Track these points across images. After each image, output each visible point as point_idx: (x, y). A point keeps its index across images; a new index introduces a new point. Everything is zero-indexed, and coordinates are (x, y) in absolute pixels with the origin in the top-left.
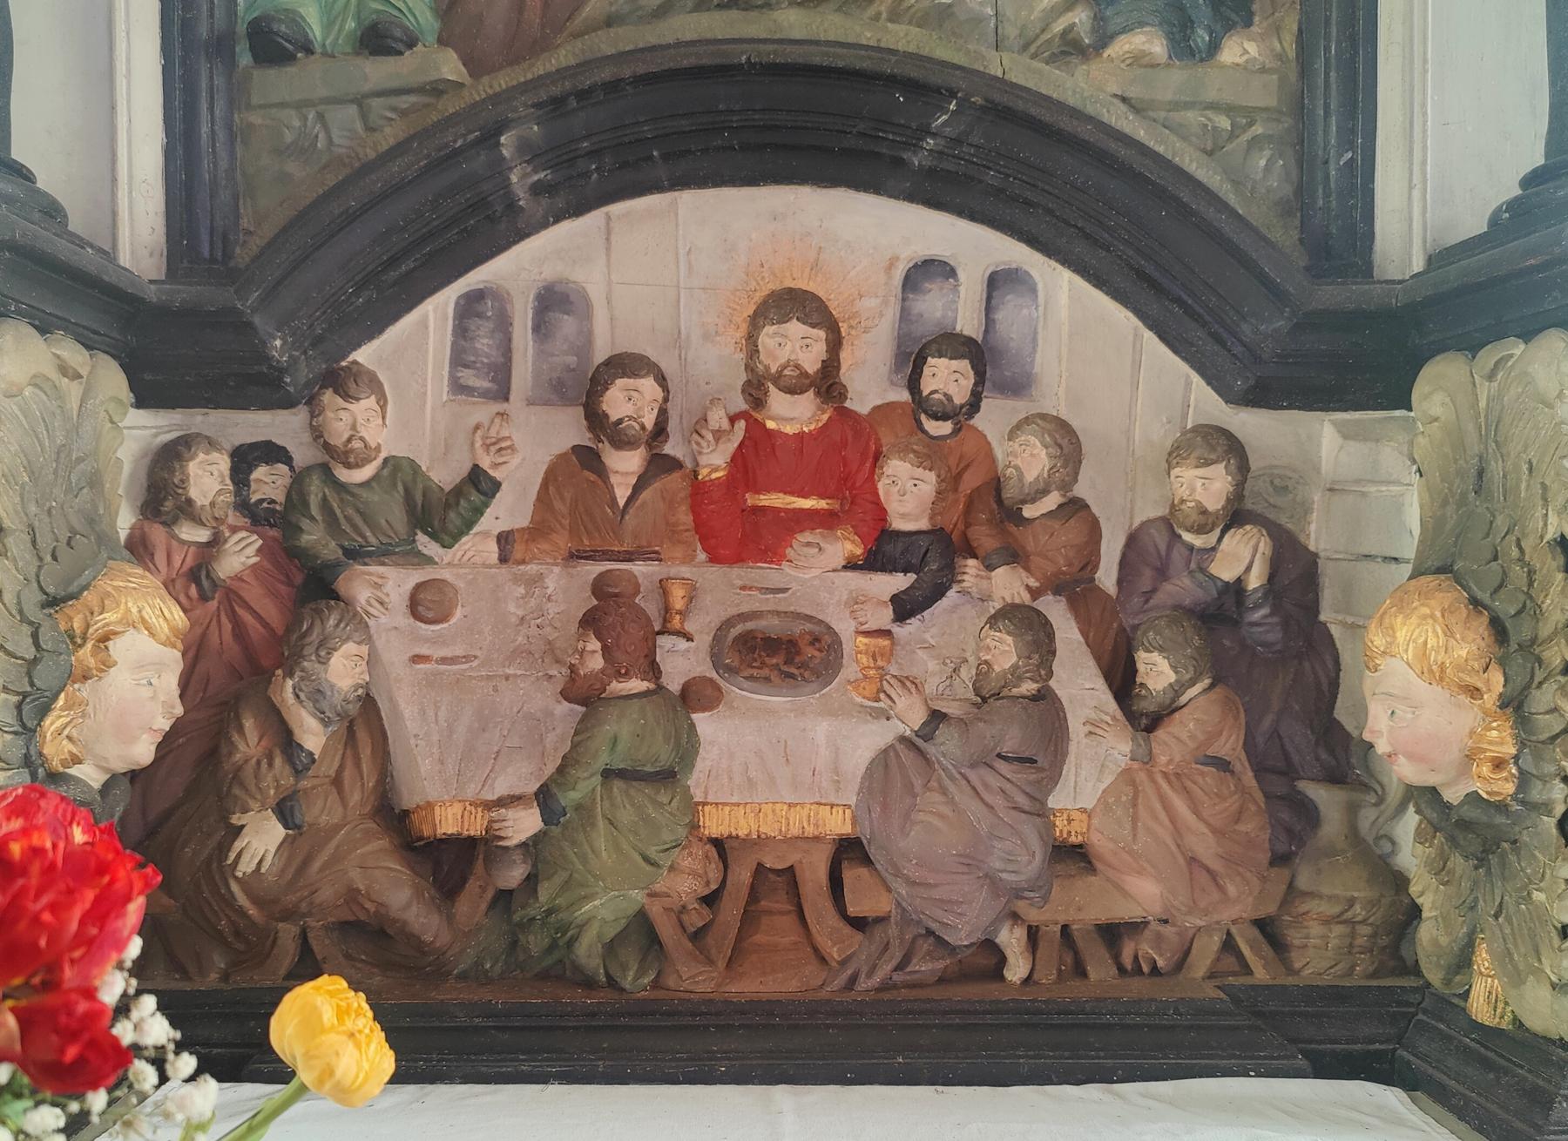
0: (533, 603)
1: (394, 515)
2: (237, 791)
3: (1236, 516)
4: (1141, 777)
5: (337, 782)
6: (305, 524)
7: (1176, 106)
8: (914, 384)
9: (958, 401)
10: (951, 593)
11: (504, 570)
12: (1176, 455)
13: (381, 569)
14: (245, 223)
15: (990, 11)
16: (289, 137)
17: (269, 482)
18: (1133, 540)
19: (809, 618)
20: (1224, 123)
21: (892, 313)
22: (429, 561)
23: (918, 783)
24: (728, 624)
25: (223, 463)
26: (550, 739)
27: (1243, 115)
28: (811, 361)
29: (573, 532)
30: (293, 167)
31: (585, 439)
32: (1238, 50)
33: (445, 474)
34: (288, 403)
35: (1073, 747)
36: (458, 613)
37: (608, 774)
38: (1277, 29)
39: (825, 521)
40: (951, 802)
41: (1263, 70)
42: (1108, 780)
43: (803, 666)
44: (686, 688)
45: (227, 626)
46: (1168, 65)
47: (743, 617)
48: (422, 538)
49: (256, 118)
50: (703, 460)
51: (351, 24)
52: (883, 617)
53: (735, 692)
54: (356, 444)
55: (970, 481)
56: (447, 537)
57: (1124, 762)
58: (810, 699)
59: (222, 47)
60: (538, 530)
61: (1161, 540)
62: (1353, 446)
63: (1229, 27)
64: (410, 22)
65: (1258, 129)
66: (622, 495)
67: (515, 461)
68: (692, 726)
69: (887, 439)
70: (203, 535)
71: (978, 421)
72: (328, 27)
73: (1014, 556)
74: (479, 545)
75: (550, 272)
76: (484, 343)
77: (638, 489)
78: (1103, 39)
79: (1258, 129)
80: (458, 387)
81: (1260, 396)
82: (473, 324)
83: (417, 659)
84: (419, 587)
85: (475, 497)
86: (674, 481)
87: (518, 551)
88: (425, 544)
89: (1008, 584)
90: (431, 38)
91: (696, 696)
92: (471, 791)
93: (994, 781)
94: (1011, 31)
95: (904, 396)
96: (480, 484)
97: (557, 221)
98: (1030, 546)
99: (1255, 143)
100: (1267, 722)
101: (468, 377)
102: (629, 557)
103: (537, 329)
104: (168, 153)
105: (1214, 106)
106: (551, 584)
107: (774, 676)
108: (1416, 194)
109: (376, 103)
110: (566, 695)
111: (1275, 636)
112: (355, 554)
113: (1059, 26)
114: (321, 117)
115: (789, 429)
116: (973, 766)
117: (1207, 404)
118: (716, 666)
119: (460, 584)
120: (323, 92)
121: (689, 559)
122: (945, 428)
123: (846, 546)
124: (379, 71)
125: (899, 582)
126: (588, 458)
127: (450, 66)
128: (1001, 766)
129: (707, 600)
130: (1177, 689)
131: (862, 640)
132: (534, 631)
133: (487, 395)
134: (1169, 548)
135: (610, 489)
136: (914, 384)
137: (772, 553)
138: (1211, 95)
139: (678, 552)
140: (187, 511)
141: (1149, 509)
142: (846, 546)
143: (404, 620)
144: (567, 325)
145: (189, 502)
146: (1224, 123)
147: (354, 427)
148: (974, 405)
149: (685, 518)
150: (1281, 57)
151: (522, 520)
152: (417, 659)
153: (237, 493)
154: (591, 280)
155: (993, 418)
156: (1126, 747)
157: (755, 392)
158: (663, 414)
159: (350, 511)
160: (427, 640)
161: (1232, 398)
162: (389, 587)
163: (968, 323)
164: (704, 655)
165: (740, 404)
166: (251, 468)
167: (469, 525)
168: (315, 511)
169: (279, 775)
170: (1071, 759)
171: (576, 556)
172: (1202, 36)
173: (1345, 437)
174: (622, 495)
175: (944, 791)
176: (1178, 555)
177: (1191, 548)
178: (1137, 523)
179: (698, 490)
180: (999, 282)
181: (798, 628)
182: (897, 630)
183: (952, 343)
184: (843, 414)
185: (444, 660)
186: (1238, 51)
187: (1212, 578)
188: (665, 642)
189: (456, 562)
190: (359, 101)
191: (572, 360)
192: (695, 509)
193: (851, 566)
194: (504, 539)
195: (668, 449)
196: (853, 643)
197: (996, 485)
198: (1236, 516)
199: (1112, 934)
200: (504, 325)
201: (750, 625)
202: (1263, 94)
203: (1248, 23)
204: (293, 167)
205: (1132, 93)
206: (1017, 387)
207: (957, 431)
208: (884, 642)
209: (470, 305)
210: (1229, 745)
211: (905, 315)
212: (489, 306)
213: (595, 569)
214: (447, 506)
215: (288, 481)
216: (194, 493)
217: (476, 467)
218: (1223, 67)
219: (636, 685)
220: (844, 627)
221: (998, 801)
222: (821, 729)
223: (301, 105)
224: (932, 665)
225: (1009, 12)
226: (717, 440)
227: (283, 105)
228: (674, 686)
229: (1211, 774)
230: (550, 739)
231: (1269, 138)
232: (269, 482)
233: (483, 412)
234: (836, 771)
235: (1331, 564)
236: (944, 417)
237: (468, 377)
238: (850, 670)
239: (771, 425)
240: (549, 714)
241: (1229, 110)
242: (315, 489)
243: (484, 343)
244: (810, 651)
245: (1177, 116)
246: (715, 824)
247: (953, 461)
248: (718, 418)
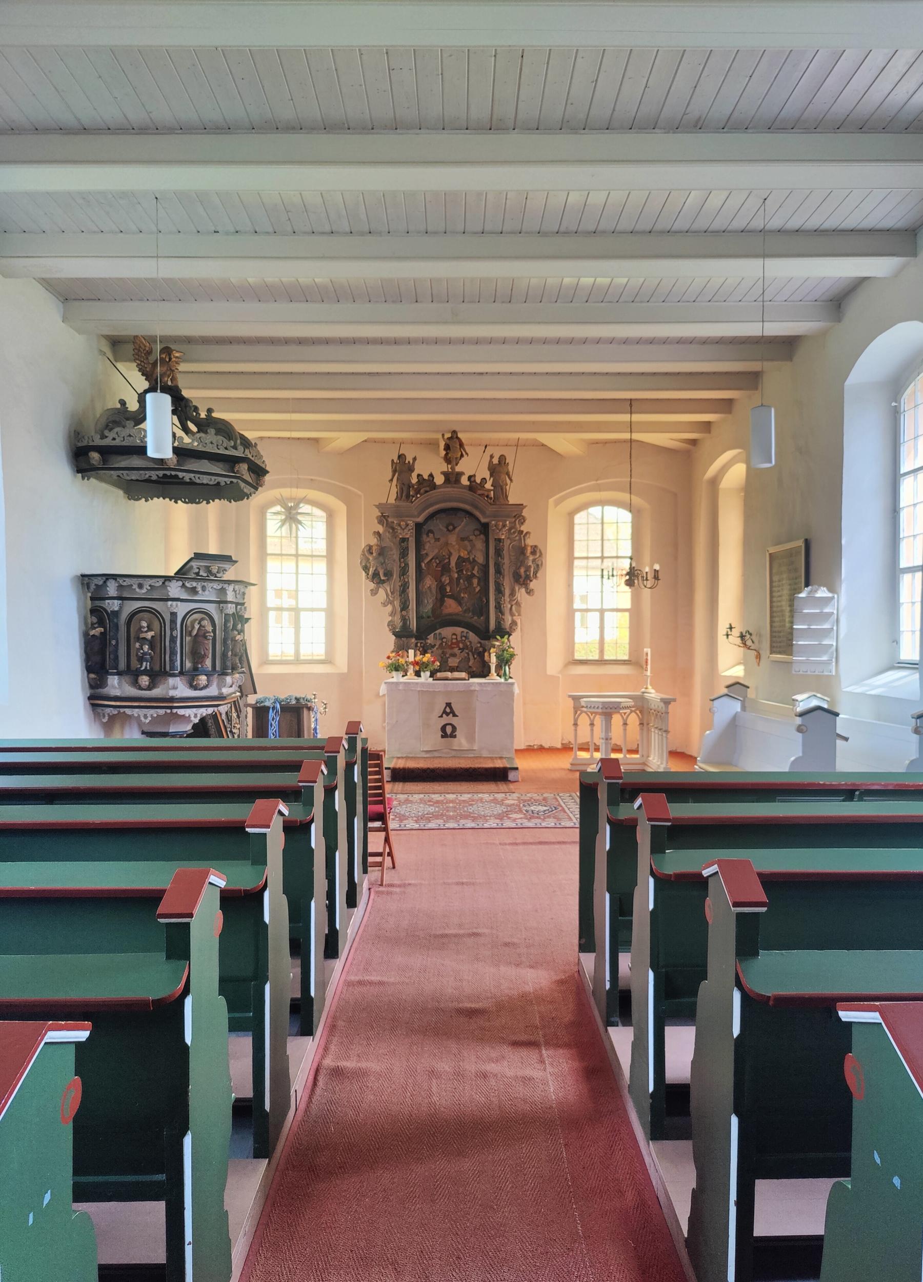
3: (481, 647)
17: (422, 645)
32: (482, 618)
73: (467, 649)
74: (435, 648)
81: (482, 640)
89: (467, 651)
91: (449, 658)
96: (435, 645)
117: (479, 640)
123: (457, 649)
126: (442, 644)
142: (457, 649)
154: (442, 632)
155: (466, 641)
157: (452, 639)
163: (465, 635)
180: (467, 633)
183: (464, 636)
198: (481, 647)
199: (473, 672)
206: (468, 639)
232: (422, 645)
246: (450, 665)
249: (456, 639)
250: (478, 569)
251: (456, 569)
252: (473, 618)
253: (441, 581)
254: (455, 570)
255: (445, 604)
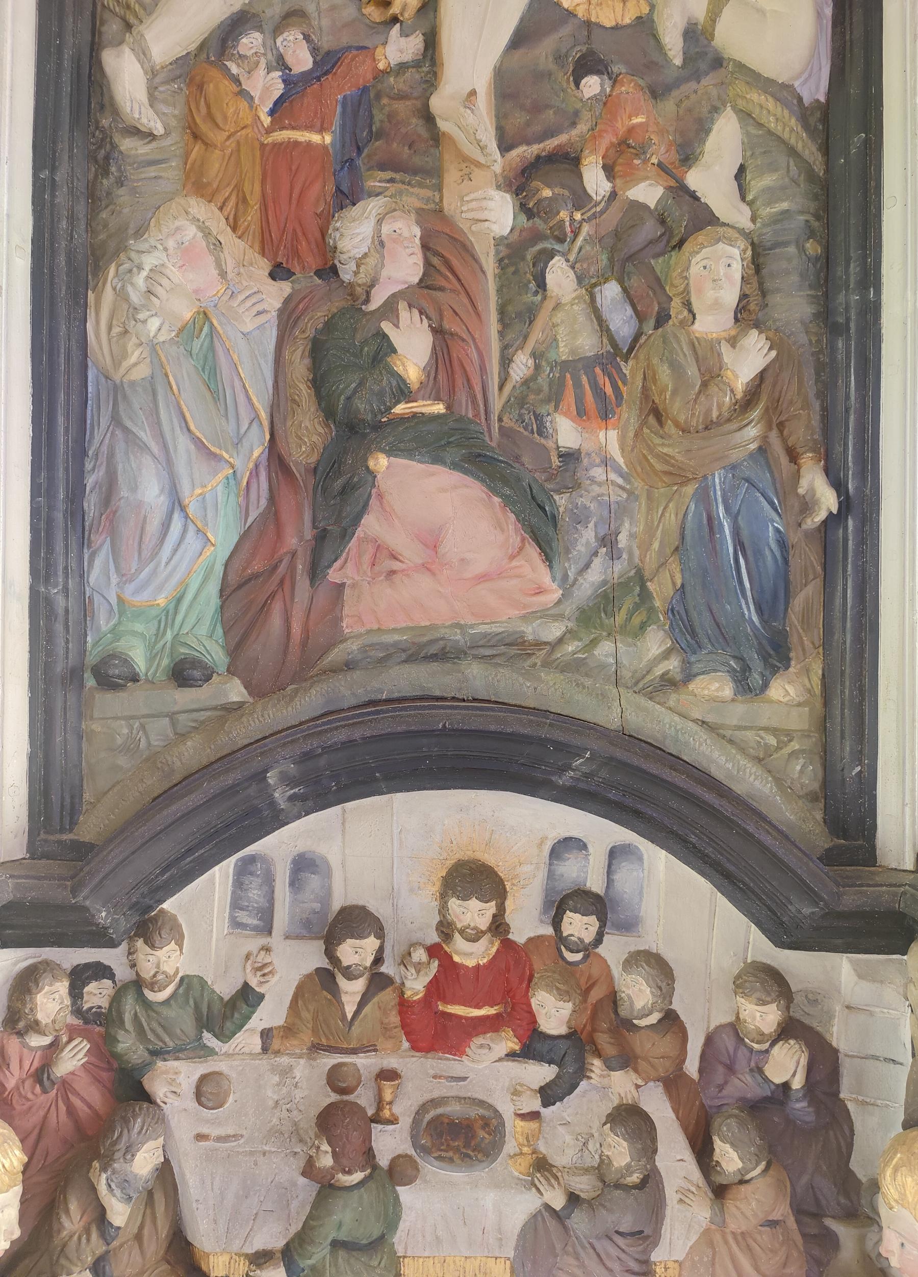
0: (284, 1090)
1: (184, 1020)
2: (63, 1261)
4: (718, 1238)
5: (138, 1237)
6: (121, 1035)
7: (739, 728)
8: (557, 923)
9: (587, 941)
10: (584, 1084)
11: (264, 1063)
12: (740, 985)
13: (176, 1064)
14: (87, 796)
15: (612, 660)
16: (119, 740)
18: (709, 1040)
19: (482, 1103)
20: (772, 741)
21: (541, 876)
22: (211, 1052)
23: (559, 1247)
24: (423, 1108)
25: (63, 987)
26: (294, 1205)
27: (784, 735)
28: (484, 922)
29: (315, 1031)
30: (122, 761)
31: (324, 963)
33: (225, 988)
34: (113, 944)
35: (668, 1212)
36: (231, 1099)
37: (336, 1244)
38: (807, 671)
39: (491, 1025)
40: (582, 1266)
41: (799, 705)
42: (694, 1238)
43: (476, 1149)
44: (394, 1161)
45: (62, 1107)
46: (733, 700)
47: (434, 1103)
48: (206, 1035)
49: (96, 727)
50: (408, 984)
51: (166, 662)
52: (535, 1104)
53: (430, 1168)
54: (160, 977)
55: (596, 994)
56: (225, 1037)
57: (705, 1224)
58: (481, 1173)
59: (74, 675)
60: (288, 1030)
61: (728, 1042)
62: (865, 984)
63: (775, 670)
64: (207, 659)
65: (795, 745)
66: (350, 1010)
67: (274, 980)
68: (397, 1198)
69: (537, 964)
70: (46, 1041)
71: (601, 950)
72: (151, 659)
75: (302, 846)
76: (255, 894)
77: (361, 1005)
78: (689, 677)
79: (795, 745)
80: (236, 924)
82: (247, 880)
83: (200, 1137)
84: (203, 1079)
85: (245, 1009)
86: (387, 996)
87: (276, 1044)
88: (209, 1039)
90: (222, 669)
92: (236, 1246)
93: (614, 1252)
94: (626, 674)
95: (549, 931)
97: (307, 814)
98: (638, 1050)
99: (793, 754)
100: (805, 1179)
101: (243, 917)
102: (354, 1052)
103: (292, 884)
104: (32, 758)
105: (766, 729)
106: (298, 1073)
107: (456, 1158)
108: (908, 810)
109: (182, 717)
110: (304, 1174)
111: (811, 1118)
112: (156, 1053)
113: (659, 671)
114: (143, 727)
115: (470, 963)
116: (598, 1238)
118: (415, 1145)
119: (233, 1075)
120: (145, 711)
121: (396, 1049)
122: (578, 957)
123: (507, 1042)
124: (185, 697)
125: (542, 1073)
127: (236, 692)
128: (620, 1241)
129: (409, 1086)
130: (742, 1172)
131: (520, 1123)
132: (285, 1114)
133: (255, 929)
134: (736, 1050)
135: (341, 1005)
136: (557, 923)
137: (457, 1049)
138: (764, 722)
139: (389, 1044)
140: (35, 1027)
141: (722, 1018)
142: (507, 1042)
143: (192, 1104)
144: (314, 882)
145: (37, 1022)
146: (772, 741)
147: (158, 966)
148: (598, 940)
149: (394, 1019)
150: (809, 691)
151: (279, 1020)
152: (200, 1137)
153: (74, 1004)
156: (708, 1215)
157: (446, 929)
158: (381, 950)
159: (154, 1025)
160: (207, 1121)
161: (780, 944)
162: (181, 1078)
163: (596, 884)
164: (406, 1135)
165: (433, 938)
166: (85, 984)
167: (241, 1027)
168: (128, 1024)
169: (96, 1246)
170: (667, 1222)
171: (316, 1048)
172: (756, 678)
173: (860, 977)
174: (350, 1010)
175: (577, 1258)
176: (742, 1053)
177: (751, 1050)
178: (712, 1027)
179: (404, 1005)
180: (615, 854)
181: (474, 1112)
182: (543, 1111)
184: (508, 945)
185: (219, 1139)
186: (781, 692)
187: (767, 1080)
188: (376, 1128)
189: (231, 1052)
190: (172, 716)
191: (317, 906)
192: (400, 1013)
193: (511, 1055)
194: (266, 1035)
195: (383, 969)
196: (515, 1129)
197: (613, 998)
200: (269, 880)
201: (440, 1111)
202: (799, 720)
203: (787, 667)
204: (122, 761)
205: (710, 718)
206: (628, 926)
207: (586, 957)
208: (533, 1125)
209: (244, 870)
210: (782, 1211)
211: (551, 875)
212: (258, 867)
213: (330, 1060)
214: (225, 1018)
215: (111, 992)
216: (40, 1016)
217: (246, 985)
218: (771, 702)
219: (358, 1176)
220: (507, 1109)
221: (616, 1267)
222: (489, 1199)
223: (128, 718)
224: (568, 1139)
225: (625, 661)
226: (418, 972)
227: (116, 718)
228: (383, 1161)
229: (765, 1236)
230: (294, 1205)
231: (802, 751)
233: (253, 944)
234: (500, 1231)
235: (848, 1060)
236: (578, 952)
237: (243, 917)
238: (510, 1146)
239: (456, 959)
240: (294, 1184)
241: (774, 731)
242: (130, 1005)
243: (255, 894)
244: (482, 1134)
245: (739, 734)
247: (583, 981)
248: (420, 955)
249: (499, 926)
250: (749, 146)
251: (505, 146)
252: (668, 683)
253: (329, 271)
254: (498, 163)
255: (371, 524)
